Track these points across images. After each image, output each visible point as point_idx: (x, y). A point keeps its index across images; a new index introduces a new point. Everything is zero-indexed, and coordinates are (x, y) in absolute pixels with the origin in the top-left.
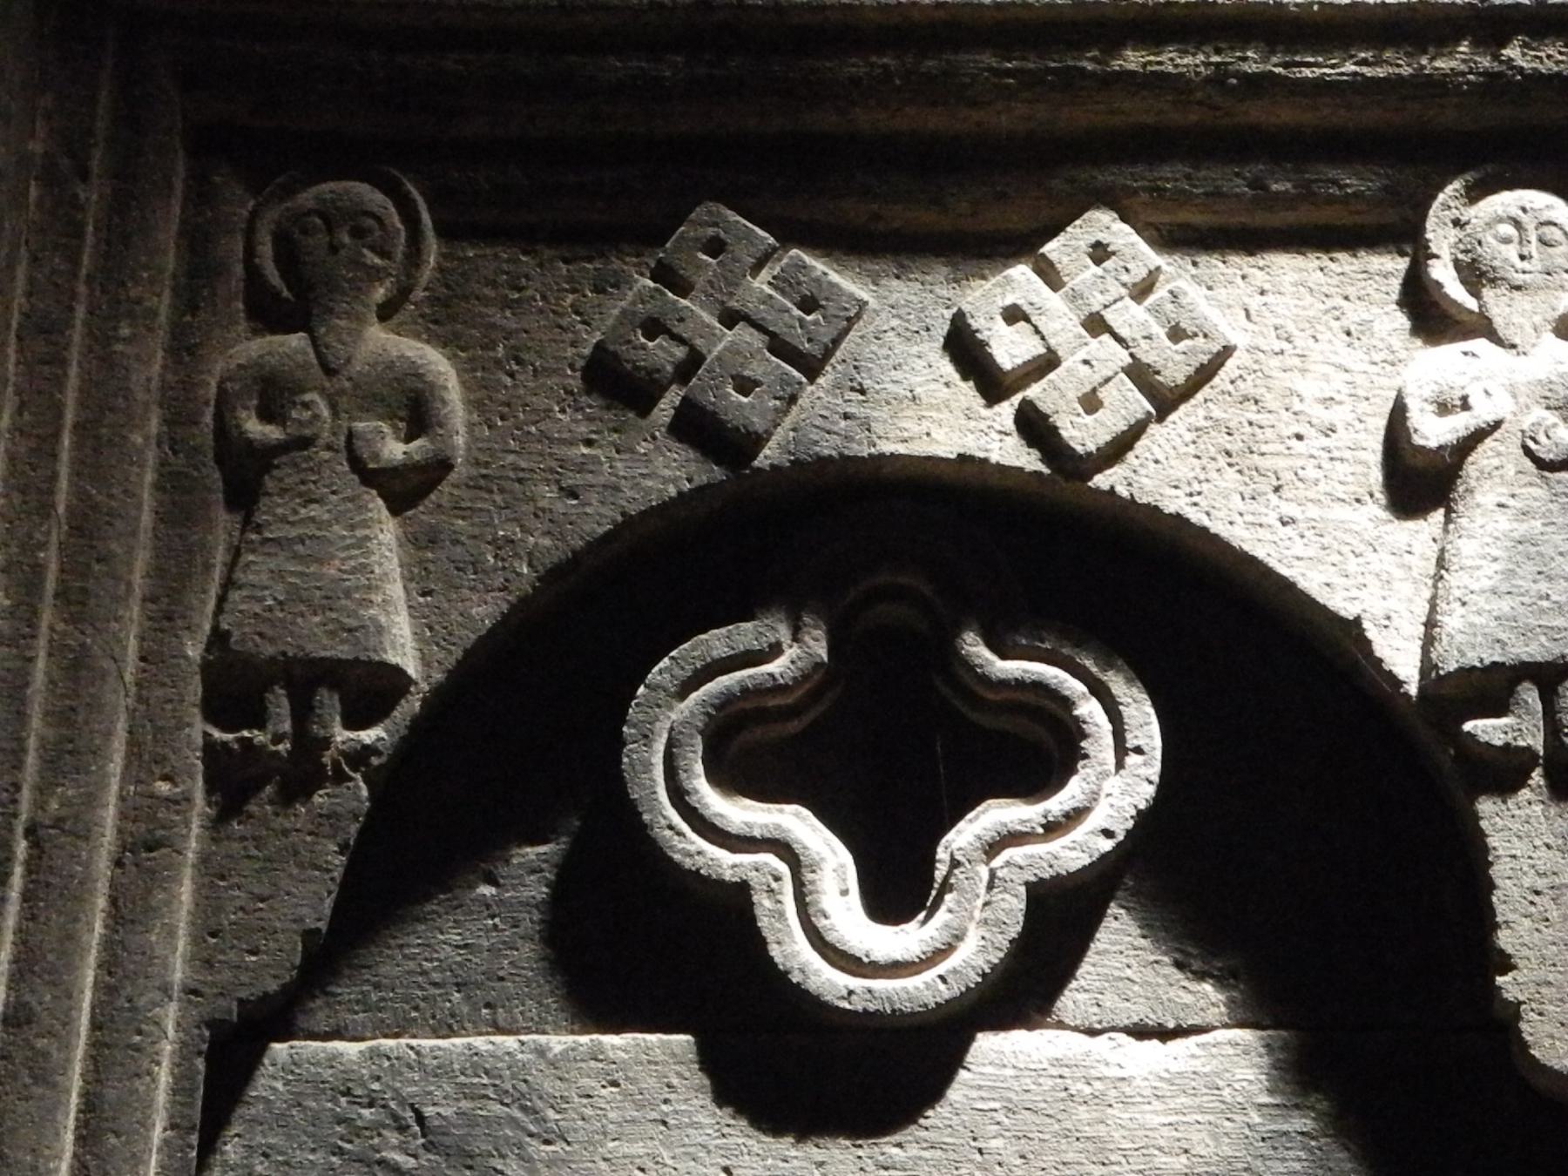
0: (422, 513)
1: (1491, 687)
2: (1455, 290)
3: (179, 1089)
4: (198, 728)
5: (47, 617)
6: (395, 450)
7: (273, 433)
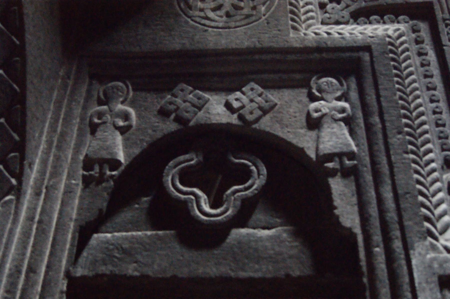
0: (127, 135)
1: (330, 157)
2: (317, 94)
3: (73, 238)
4: (81, 172)
5: (53, 150)
6: (121, 123)
7: (99, 121)
